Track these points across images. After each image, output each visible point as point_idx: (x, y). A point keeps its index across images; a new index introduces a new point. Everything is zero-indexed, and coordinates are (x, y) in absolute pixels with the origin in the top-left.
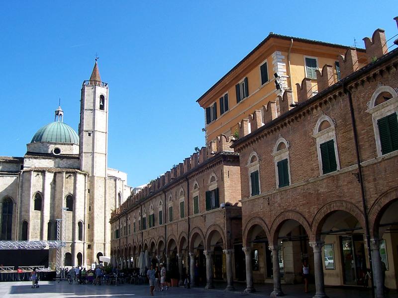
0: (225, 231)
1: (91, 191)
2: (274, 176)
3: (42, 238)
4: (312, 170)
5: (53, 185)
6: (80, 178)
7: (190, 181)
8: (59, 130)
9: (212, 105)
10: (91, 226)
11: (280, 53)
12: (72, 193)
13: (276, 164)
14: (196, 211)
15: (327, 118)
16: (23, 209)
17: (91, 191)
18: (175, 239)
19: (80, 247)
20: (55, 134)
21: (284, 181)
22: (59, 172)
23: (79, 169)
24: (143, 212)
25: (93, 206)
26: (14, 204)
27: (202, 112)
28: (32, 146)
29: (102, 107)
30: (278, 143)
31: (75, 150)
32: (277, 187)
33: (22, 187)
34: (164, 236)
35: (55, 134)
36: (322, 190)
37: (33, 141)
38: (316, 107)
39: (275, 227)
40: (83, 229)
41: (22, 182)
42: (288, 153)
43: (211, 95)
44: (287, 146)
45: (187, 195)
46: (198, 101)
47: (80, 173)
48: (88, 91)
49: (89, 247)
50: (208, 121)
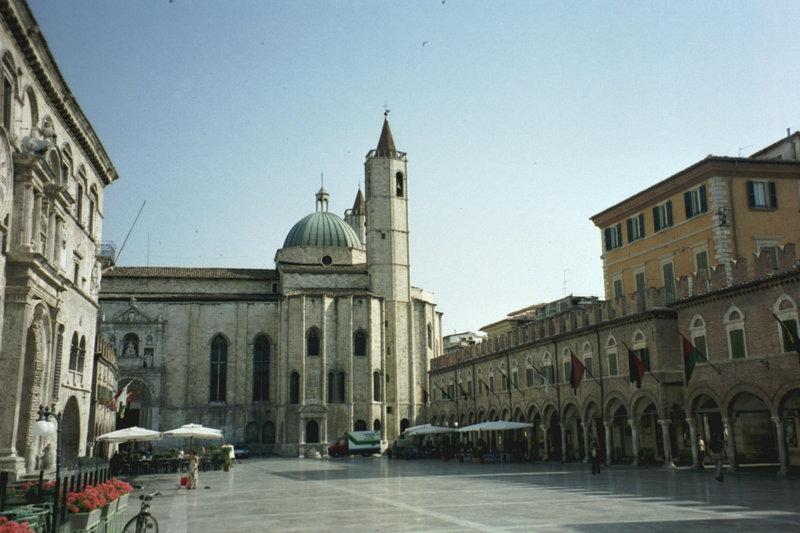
0: (660, 400)
1: (388, 324)
2: (726, 345)
3: (321, 398)
4: (773, 345)
5: (334, 316)
6: (375, 304)
7: (601, 333)
8: (327, 227)
9: (613, 226)
10: (391, 378)
11: (719, 179)
12: (364, 327)
13: (728, 332)
14: (614, 371)
15: (788, 298)
16: (291, 354)
17: (388, 324)
18: (575, 403)
19: (377, 410)
20: (321, 232)
21: (738, 351)
22: (343, 297)
23: (367, 290)
24: (511, 364)
25: (394, 348)
26: (272, 347)
27: (596, 234)
28: (287, 252)
29: (400, 193)
30: (730, 311)
31: (358, 258)
32: (731, 357)
33: (287, 320)
34: (557, 399)
35: (321, 232)
36: (783, 367)
37: (285, 246)
38: (777, 285)
39: (729, 399)
40: (383, 380)
41: (287, 312)
42: (743, 323)
43: (613, 214)
44: (742, 317)
45: (596, 350)
46: (593, 218)
47: (375, 298)
48: (377, 165)
49: (390, 410)
50: (608, 246)
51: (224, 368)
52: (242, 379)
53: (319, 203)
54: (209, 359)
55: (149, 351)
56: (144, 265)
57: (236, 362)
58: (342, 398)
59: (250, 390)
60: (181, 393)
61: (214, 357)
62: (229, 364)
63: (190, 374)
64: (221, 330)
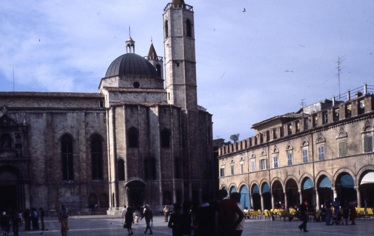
5: (146, 121)
51: (71, 157)
52: (84, 165)
53: (128, 48)
54: (60, 152)
55: (19, 146)
56: (13, 91)
57: (79, 153)
58: (154, 176)
59: (90, 173)
60: (42, 175)
61: (63, 149)
62: (74, 155)
63: (49, 162)
64: (68, 131)
